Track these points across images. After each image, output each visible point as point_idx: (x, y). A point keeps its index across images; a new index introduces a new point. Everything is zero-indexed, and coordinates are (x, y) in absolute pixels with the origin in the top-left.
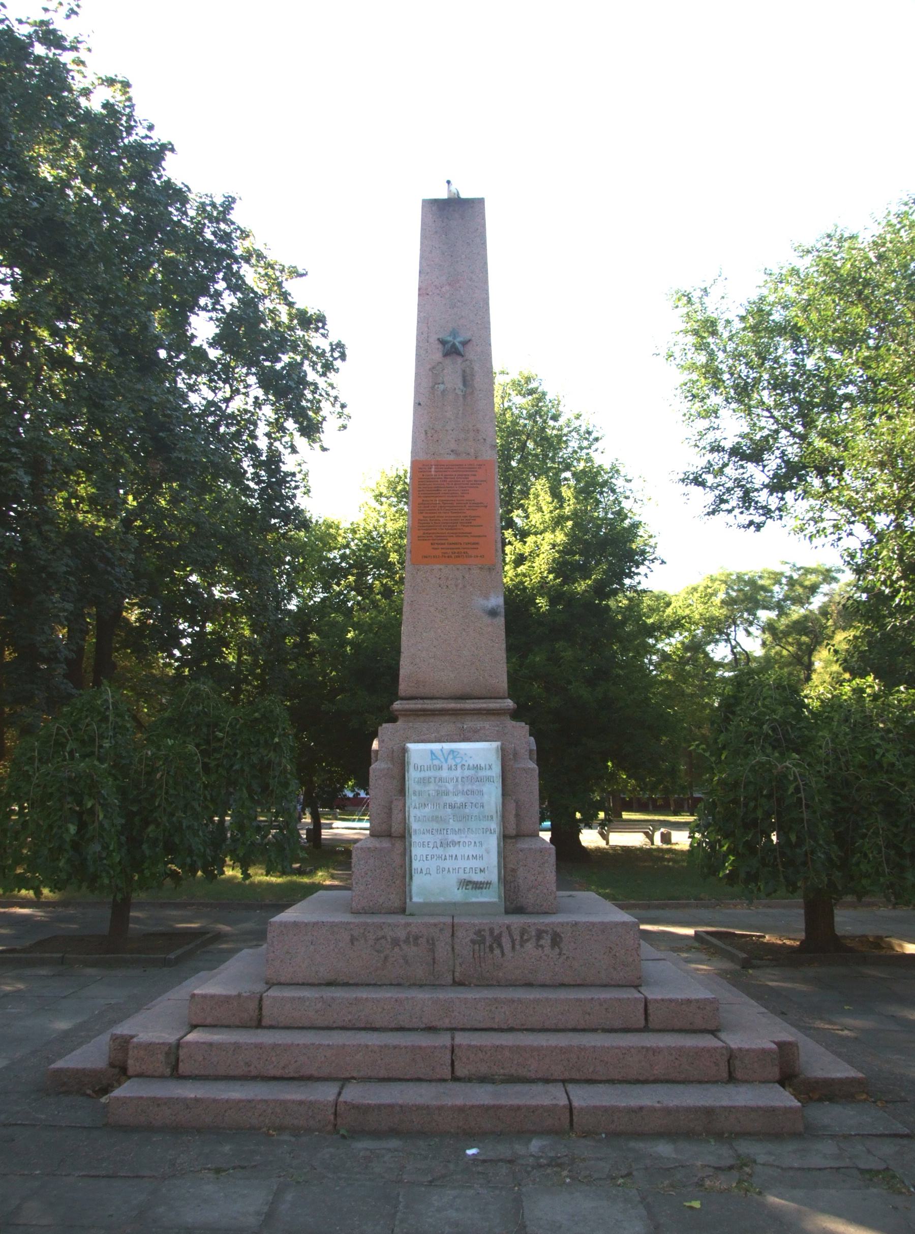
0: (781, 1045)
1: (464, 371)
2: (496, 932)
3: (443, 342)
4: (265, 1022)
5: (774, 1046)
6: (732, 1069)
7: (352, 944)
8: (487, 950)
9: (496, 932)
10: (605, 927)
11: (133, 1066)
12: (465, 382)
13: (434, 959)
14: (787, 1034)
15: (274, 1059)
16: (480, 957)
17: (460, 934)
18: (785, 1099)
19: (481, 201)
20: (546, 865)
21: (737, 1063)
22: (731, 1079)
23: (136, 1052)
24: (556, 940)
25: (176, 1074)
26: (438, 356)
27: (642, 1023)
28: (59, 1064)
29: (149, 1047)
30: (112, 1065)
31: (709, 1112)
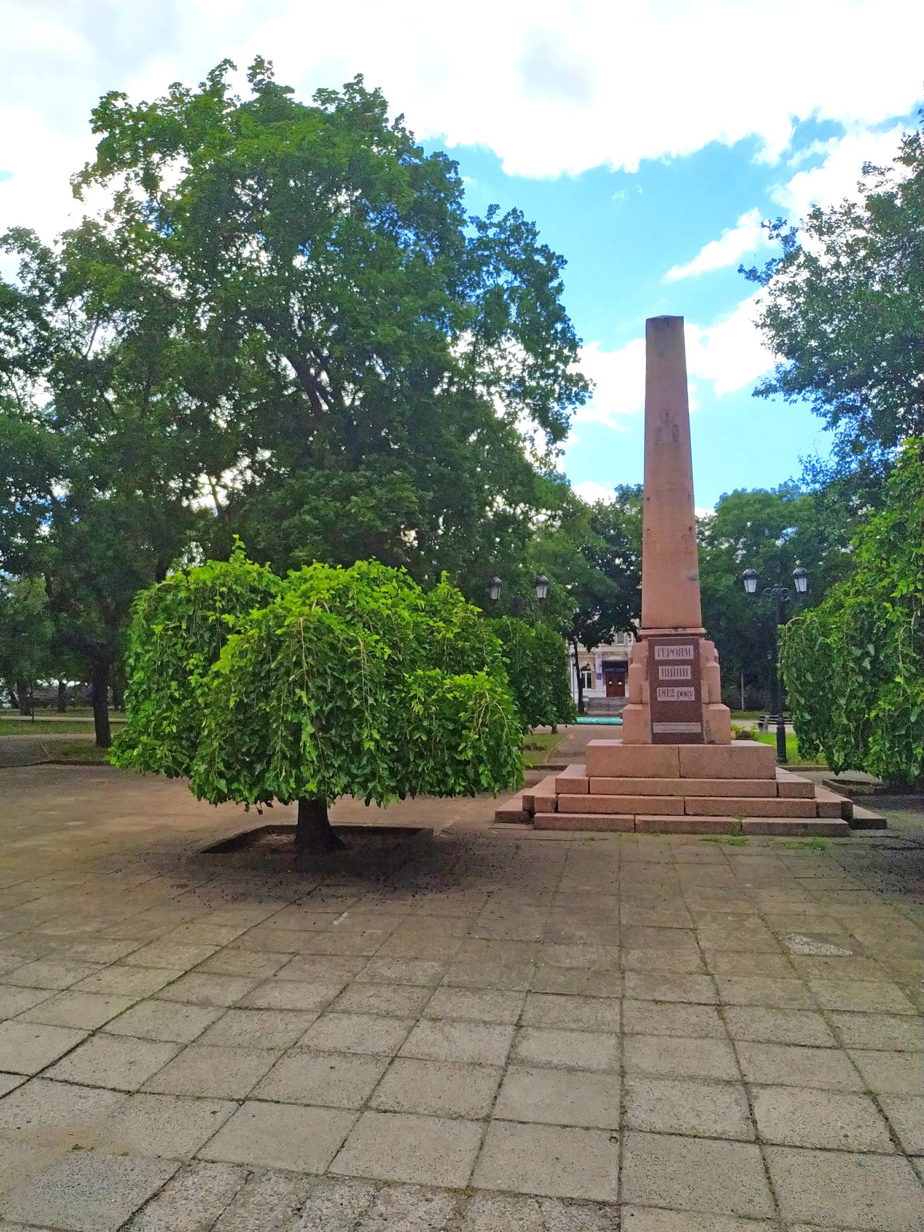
22: (818, 816)
25: (556, 811)
28: (500, 809)
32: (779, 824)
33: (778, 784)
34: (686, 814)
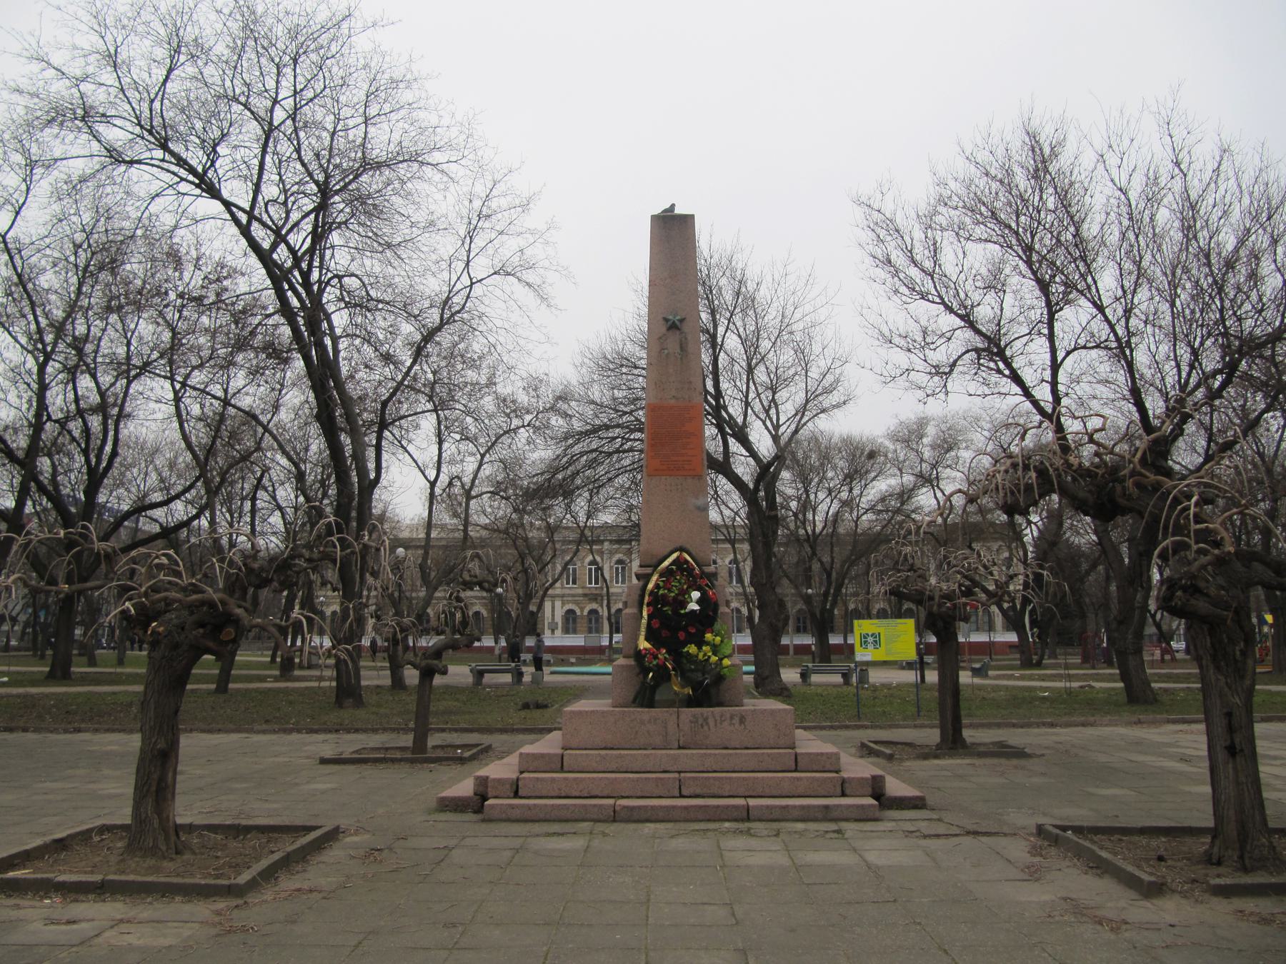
0: (874, 778)
3: (666, 320)
4: (565, 768)
10: (773, 712)
11: (491, 792)
12: (682, 348)
17: (683, 717)
19: (692, 216)
22: (843, 795)
24: (742, 720)
25: (516, 795)
26: (664, 329)
27: (793, 767)
28: (444, 794)
29: (499, 781)
30: (475, 794)
31: (827, 807)
32: (795, 807)
33: (796, 755)
34: (682, 796)
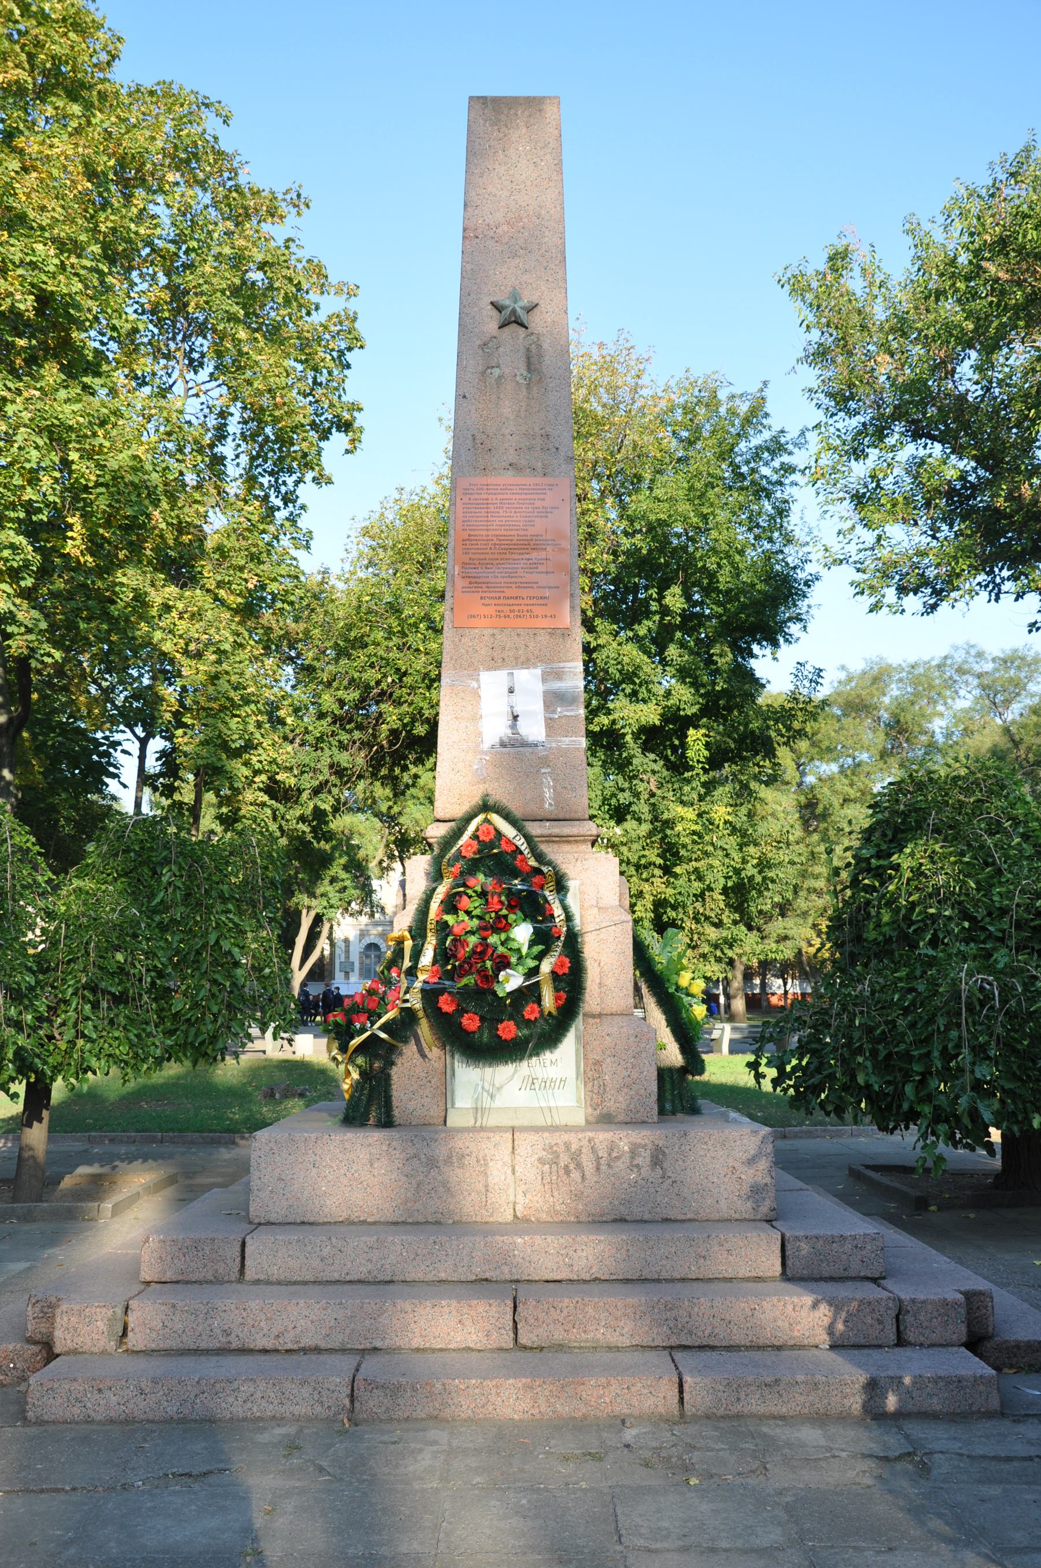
1: (528, 350)
2: (574, 1147)
5: (960, 1296)
6: (902, 1328)
7: (371, 1165)
8: (562, 1172)
9: (574, 1147)
13: (486, 1186)
14: (980, 1284)
15: (263, 1324)
16: (551, 1183)
17: (521, 1151)
18: (973, 1366)
20: (644, 1055)
21: (909, 1319)
23: (65, 1319)
